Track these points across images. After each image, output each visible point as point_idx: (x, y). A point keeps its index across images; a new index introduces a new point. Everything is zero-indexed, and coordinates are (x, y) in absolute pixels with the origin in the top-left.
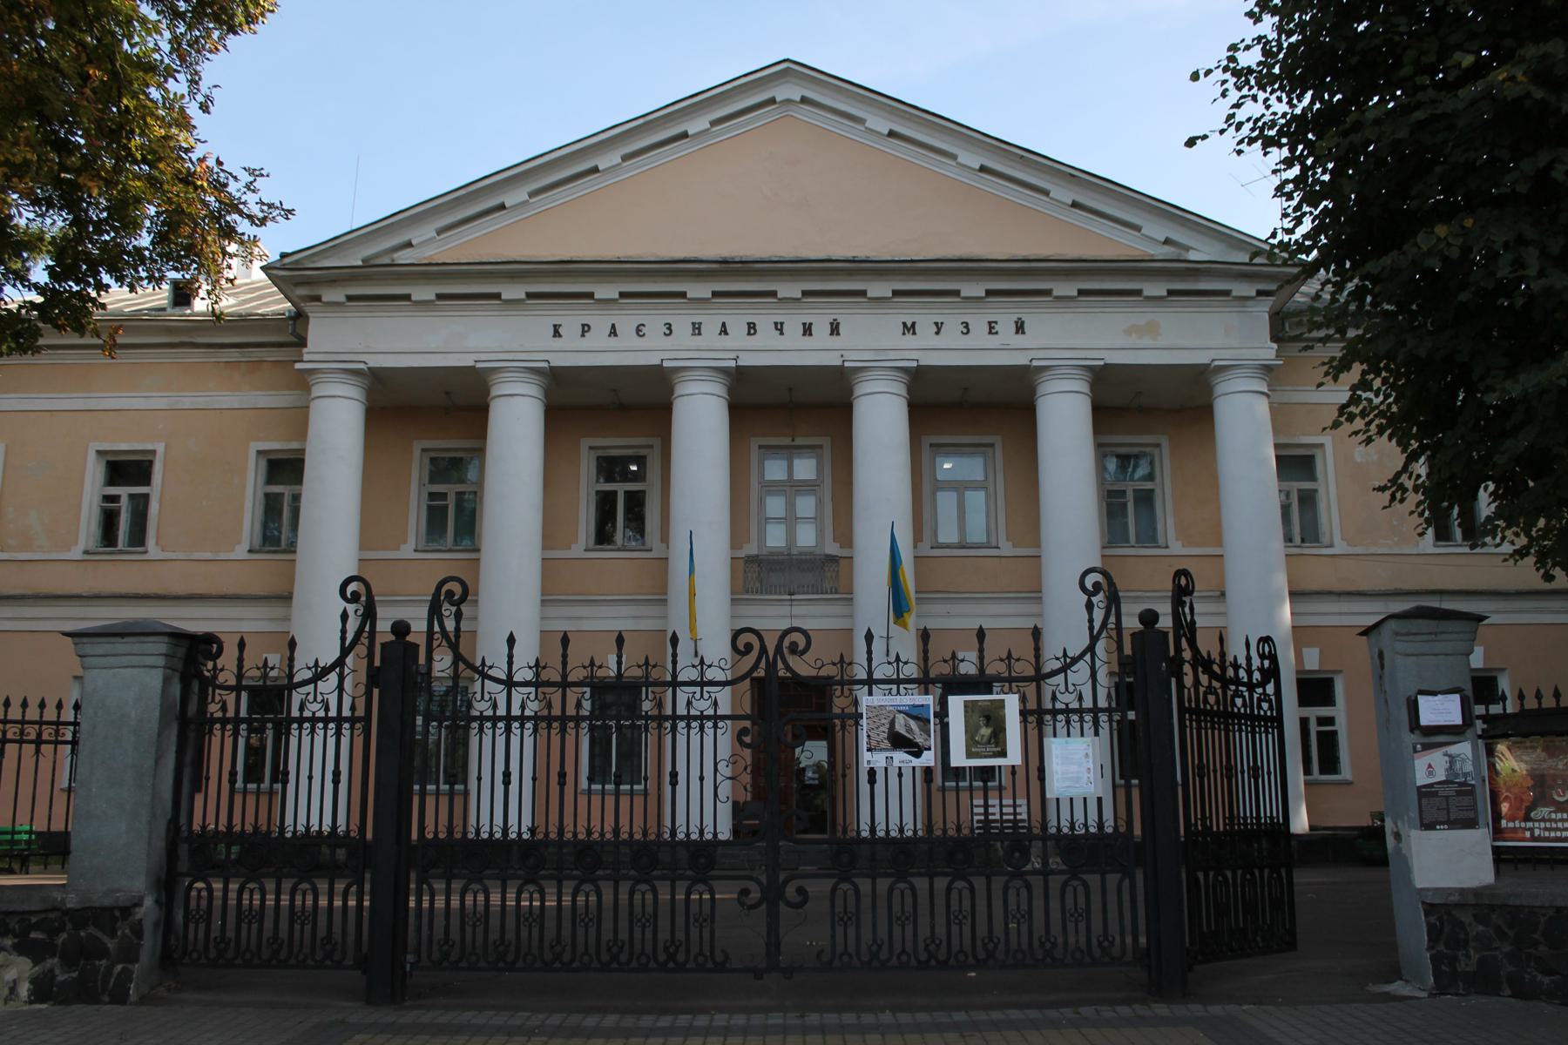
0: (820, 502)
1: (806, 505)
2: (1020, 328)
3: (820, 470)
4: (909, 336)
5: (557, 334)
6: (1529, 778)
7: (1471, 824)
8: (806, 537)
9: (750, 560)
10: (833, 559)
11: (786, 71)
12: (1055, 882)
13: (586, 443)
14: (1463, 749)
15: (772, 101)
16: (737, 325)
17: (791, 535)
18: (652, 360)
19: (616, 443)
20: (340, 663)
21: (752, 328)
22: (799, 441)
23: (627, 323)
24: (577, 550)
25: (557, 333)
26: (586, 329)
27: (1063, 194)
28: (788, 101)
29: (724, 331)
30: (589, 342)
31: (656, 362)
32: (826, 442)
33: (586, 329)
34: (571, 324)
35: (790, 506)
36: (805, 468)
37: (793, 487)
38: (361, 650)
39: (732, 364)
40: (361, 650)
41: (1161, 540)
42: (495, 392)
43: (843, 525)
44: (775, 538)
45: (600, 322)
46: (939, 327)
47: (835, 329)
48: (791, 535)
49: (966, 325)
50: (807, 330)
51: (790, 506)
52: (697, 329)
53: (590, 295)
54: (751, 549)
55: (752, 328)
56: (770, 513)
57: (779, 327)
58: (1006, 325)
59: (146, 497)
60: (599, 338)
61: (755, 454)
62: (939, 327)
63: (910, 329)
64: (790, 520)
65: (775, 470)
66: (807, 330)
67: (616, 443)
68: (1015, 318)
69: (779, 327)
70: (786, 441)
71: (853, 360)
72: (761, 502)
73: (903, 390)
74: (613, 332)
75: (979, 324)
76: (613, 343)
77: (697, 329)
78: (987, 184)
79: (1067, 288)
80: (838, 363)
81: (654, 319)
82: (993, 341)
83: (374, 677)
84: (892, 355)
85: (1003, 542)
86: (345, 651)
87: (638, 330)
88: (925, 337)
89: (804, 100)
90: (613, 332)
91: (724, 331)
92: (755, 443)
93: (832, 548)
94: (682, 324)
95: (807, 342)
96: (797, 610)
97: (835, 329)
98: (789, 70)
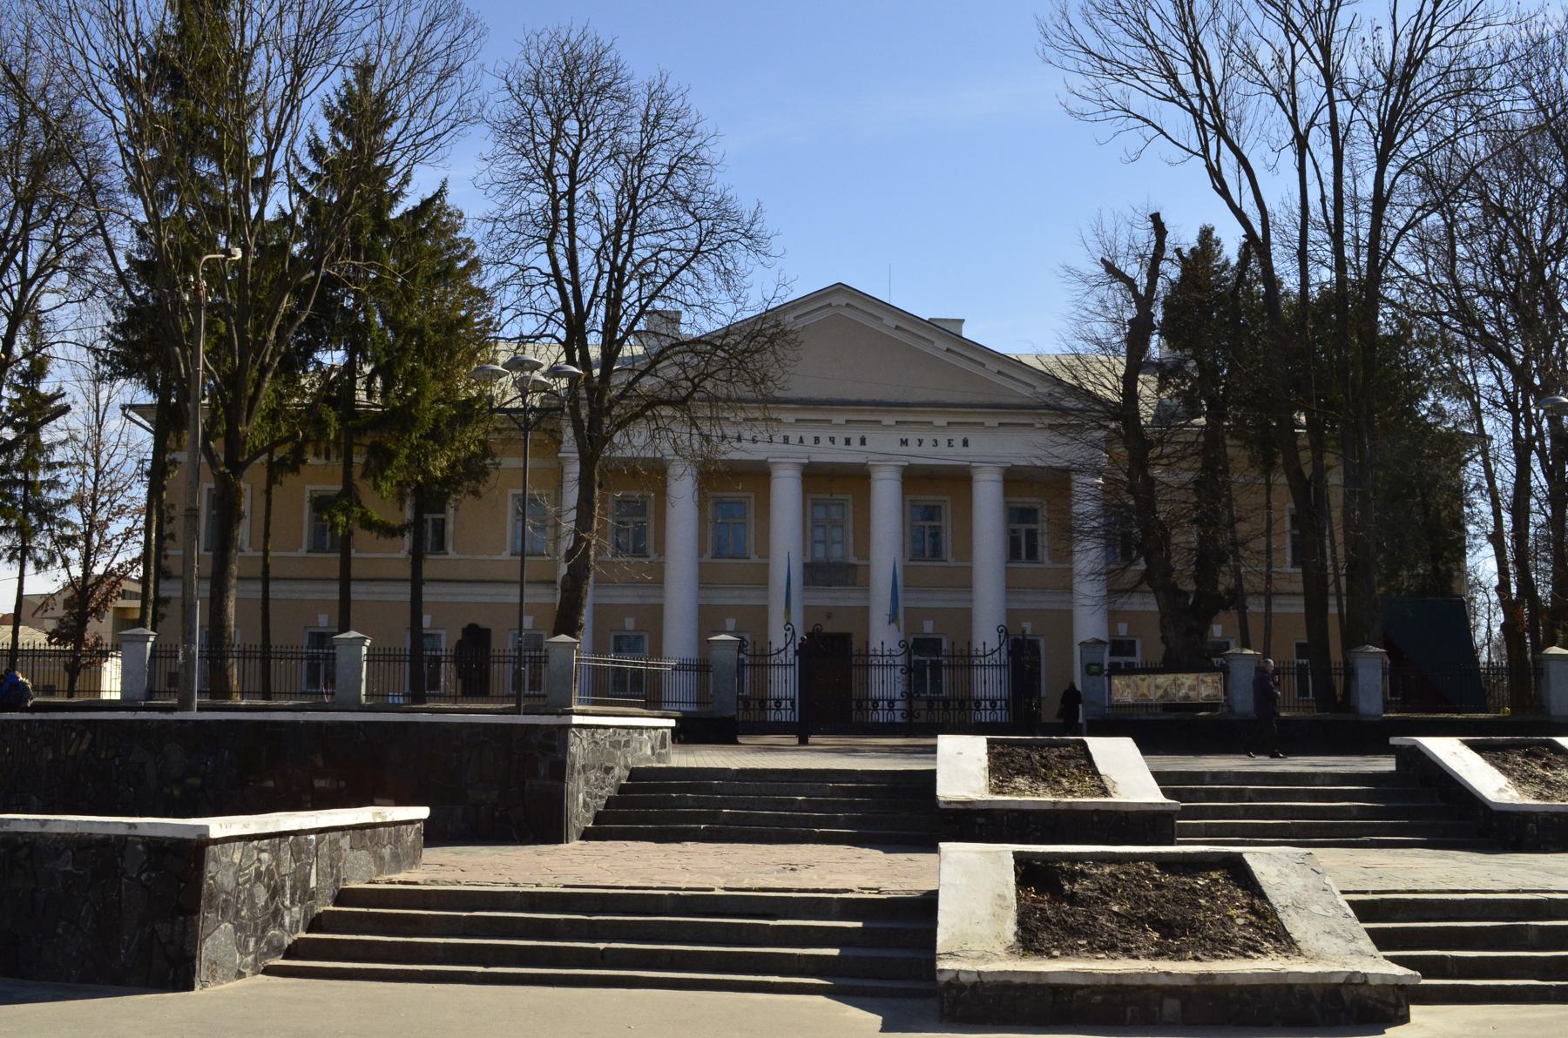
2: (965, 443)
4: (904, 447)
6: (1160, 692)
8: (837, 553)
10: (854, 566)
11: (839, 289)
18: (761, 457)
22: (835, 497)
27: (993, 366)
32: (850, 497)
39: (806, 461)
41: (1040, 558)
46: (921, 442)
47: (863, 442)
49: (936, 441)
57: (832, 440)
59: (443, 521)
62: (921, 442)
63: (904, 442)
66: (848, 442)
79: (992, 422)
80: (864, 461)
88: (913, 448)
89: (847, 305)
93: (853, 560)
97: (863, 442)
98: (840, 288)
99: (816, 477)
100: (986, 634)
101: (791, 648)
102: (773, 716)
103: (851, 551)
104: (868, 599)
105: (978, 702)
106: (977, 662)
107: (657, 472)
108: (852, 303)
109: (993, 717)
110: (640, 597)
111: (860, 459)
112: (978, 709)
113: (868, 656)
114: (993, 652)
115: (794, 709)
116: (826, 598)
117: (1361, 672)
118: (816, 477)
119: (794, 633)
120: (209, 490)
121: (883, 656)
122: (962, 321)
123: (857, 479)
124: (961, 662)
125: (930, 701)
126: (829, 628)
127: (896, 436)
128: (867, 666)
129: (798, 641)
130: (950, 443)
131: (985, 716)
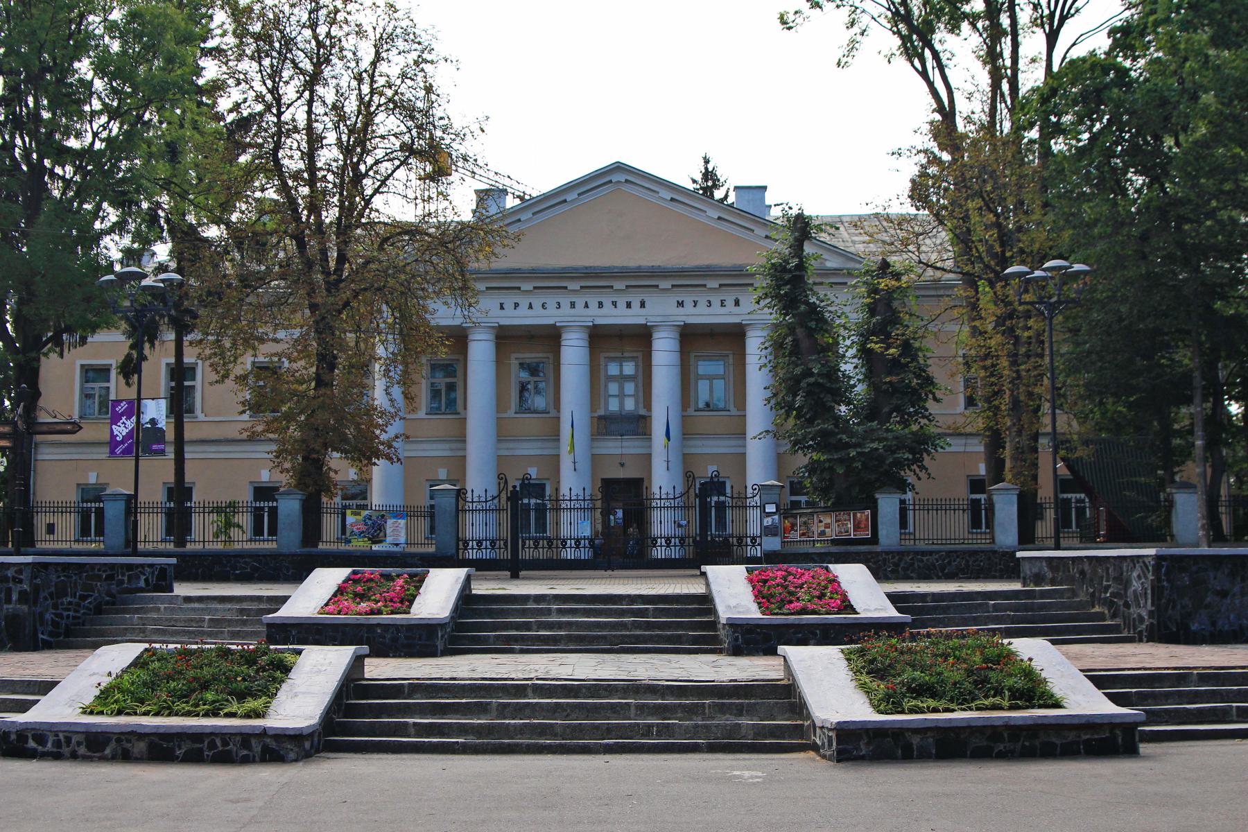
0: (636, 386)
1: (630, 388)
3: (637, 370)
5: (502, 308)
7: (776, 535)
8: (630, 405)
9: (600, 418)
12: (677, 548)
13: (513, 356)
14: (776, 517)
15: (611, 182)
16: (593, 303)
17: (622, 404)
18: (550, 321)
19: (530, 356)
20: (499, 495)
21: (601, 305)
22: (626, 355)
23: (537, 303)
24: (511, 413)
25: (502, 308)
26: (516, 305)
28: (619, 182)
29: (587, 306)
30: (519, 312)
31: (551, 322)
33: (516, 305)
34: (509, 302)
35: (621, 388)
36: (629, 369)
37: (622, 379)
38: (504, 492)
39: (591, 324)
40: (504, 492)
42: (471, 337)
43: (648, 405)
44: (614, 406)
45: (524, 303)
46: (695, 303)
47: (643, 305)
48: (622, 404)
49: (709, 302)
50: (629, 305)
51: (621, 388)
52: (573, 305)
53: (519, 288)
54: (601, 412)
55: (601, 305)
56: (611, 392)
57: (615, 304)
58: (730, 302)
60: (523, 310)
61: (602, 362)
62: (695, 303)
63: (681, 304)
64: (621, 396)
65: (613, 369)
66: (629, 305)
67: (530, 356)
68: (734, 298)
69: (615, 304)
70: (619, 355)
71: (651, 321)
72: (606, 386)
73: (677, 336)
74: (531, 307)
75: (716, 302)
76: (530, 312)
77: (573, 305)
78: (723, 226)
81: (551, 301)
82: (723, 310)
83: (508, 499)
84: (672, 318)
85: (732, 407)
86: (500, 492)
87: (543, 306)
89: (627, 181)
90: (531, 307)
91: (587, 306)
92: (603, 355)
93: (642, 412)
94: (565, 303)
95: (629, 311)
96: (625, 444)
97: (643, 305)
98: (619, 167)
99: (506, 338)
100: (479, 482)
101: (503, 495)
102: (569, 554)
103: (641, 405)
104: (650, 447)
105: (564, 541)
106: (563, 506)
107: (459, 339)
108: (629, 178)
109: (578, 554)
110: (451, 450)
111: (642, 321)
112: (564, 547)
113: (557, 500)
114: (494, 498)
115: (506, 547)
116: (612, 447)
117: (997, 507)
118: (506, 338)
119: (506, 482)
120: (168, 364)
121: (570, 500)
122: (764, 188)
123: (641, 337)
124: (479, 507)
125: (536, 541)
126: (621, 474)
127: (673, 301)
128: (557, 509)
129: (510, 488)
130: (722, 304)
131: (472, 554)
